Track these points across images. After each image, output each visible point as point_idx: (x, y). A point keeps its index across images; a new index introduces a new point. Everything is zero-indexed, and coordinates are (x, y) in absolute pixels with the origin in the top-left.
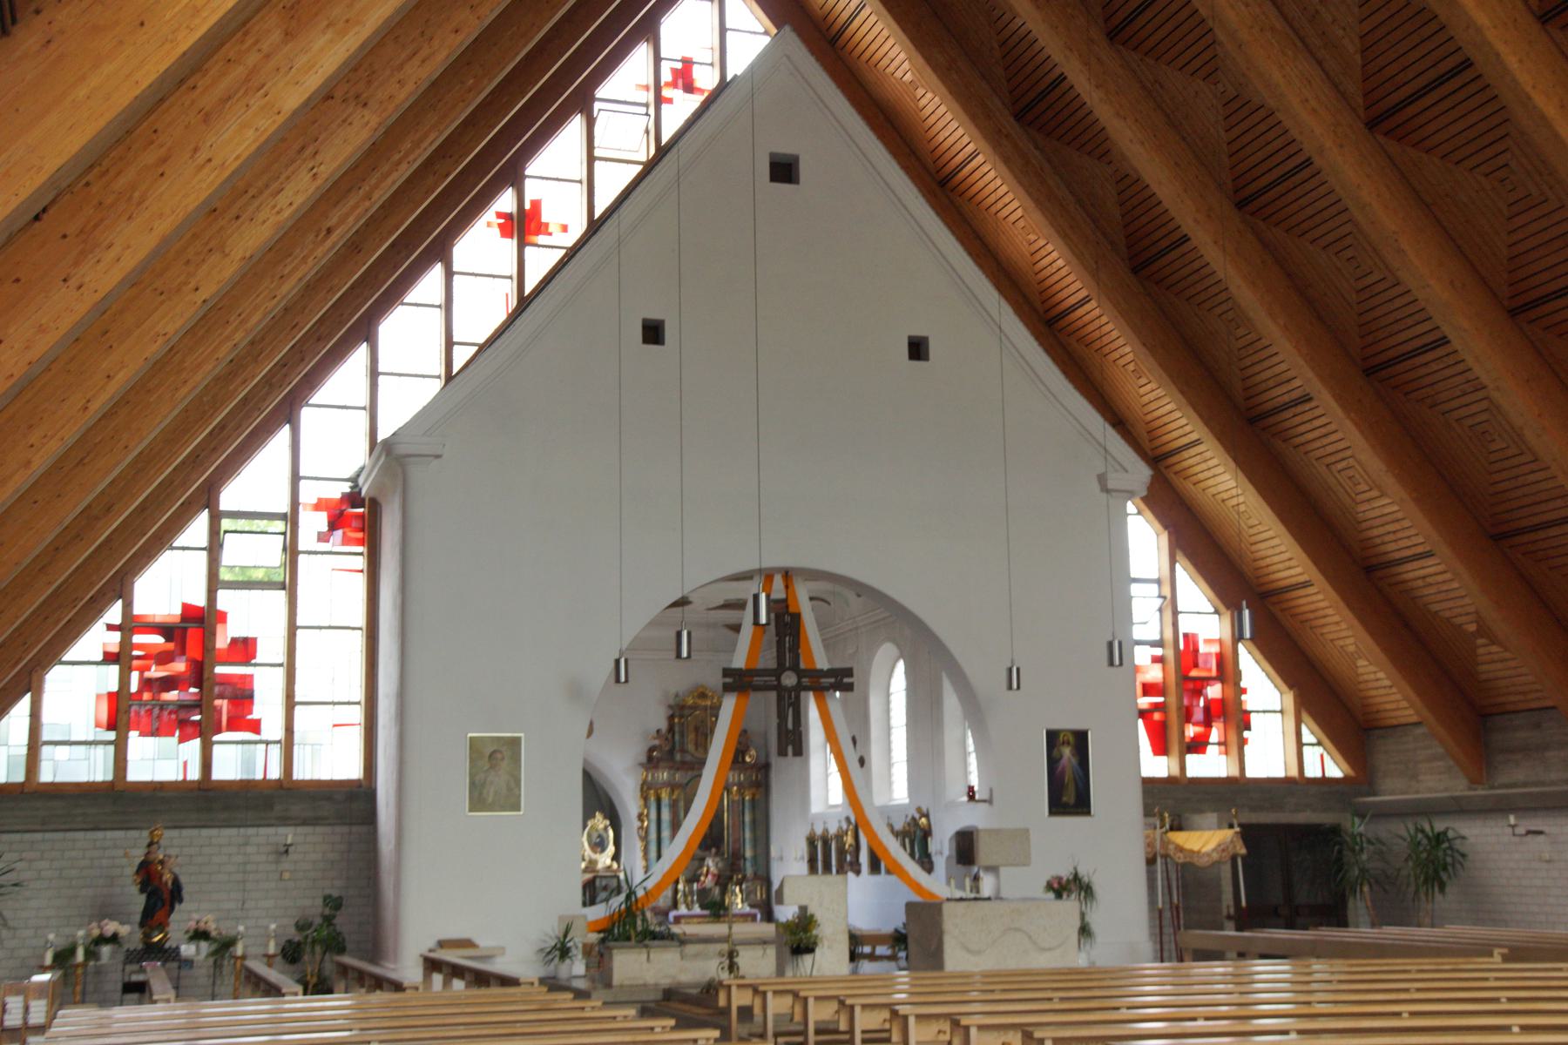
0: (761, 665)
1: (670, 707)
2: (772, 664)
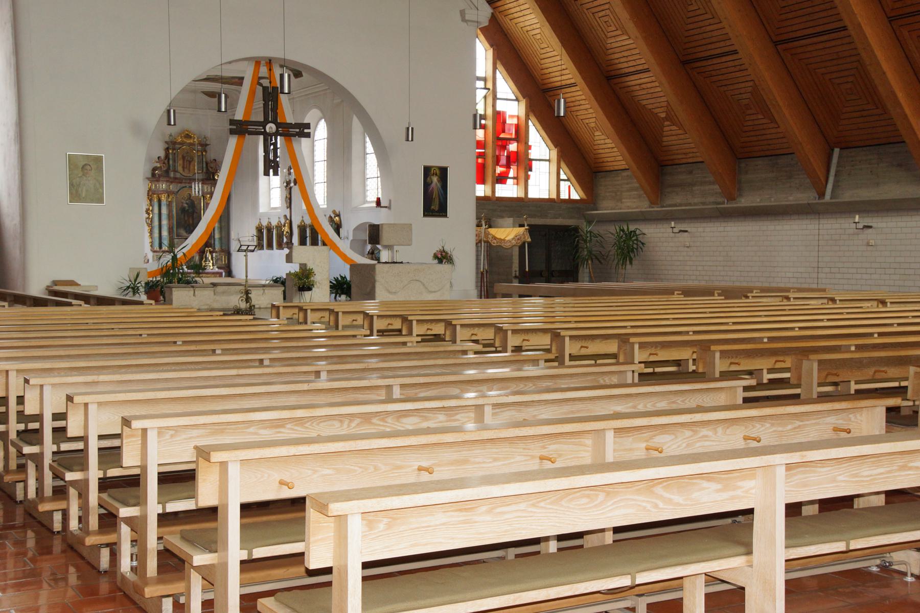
0: (253, 119)
1: (166, 142)
2: (261, 118)
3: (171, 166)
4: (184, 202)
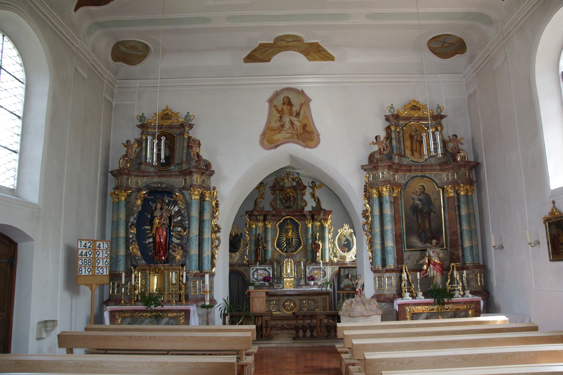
1: (387, 119)
3: (395, 147)
4: (416, 197)
